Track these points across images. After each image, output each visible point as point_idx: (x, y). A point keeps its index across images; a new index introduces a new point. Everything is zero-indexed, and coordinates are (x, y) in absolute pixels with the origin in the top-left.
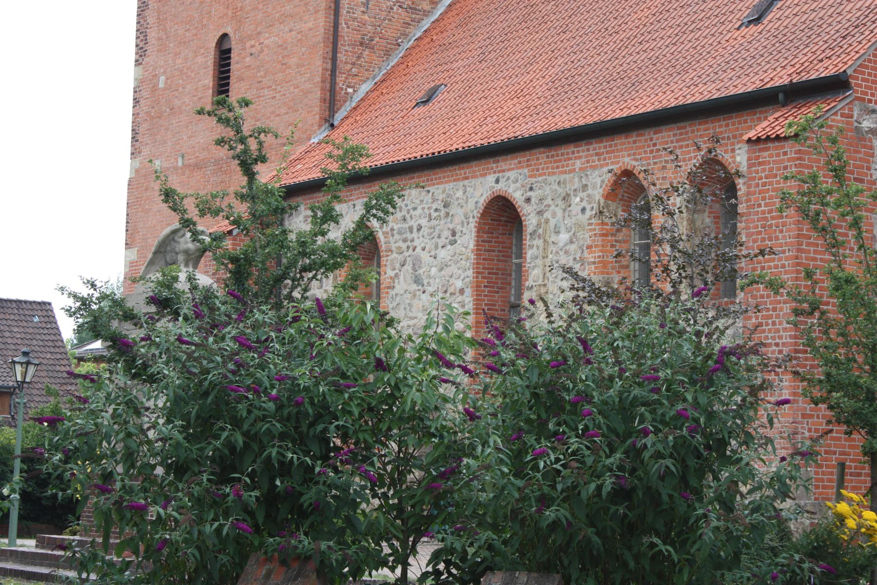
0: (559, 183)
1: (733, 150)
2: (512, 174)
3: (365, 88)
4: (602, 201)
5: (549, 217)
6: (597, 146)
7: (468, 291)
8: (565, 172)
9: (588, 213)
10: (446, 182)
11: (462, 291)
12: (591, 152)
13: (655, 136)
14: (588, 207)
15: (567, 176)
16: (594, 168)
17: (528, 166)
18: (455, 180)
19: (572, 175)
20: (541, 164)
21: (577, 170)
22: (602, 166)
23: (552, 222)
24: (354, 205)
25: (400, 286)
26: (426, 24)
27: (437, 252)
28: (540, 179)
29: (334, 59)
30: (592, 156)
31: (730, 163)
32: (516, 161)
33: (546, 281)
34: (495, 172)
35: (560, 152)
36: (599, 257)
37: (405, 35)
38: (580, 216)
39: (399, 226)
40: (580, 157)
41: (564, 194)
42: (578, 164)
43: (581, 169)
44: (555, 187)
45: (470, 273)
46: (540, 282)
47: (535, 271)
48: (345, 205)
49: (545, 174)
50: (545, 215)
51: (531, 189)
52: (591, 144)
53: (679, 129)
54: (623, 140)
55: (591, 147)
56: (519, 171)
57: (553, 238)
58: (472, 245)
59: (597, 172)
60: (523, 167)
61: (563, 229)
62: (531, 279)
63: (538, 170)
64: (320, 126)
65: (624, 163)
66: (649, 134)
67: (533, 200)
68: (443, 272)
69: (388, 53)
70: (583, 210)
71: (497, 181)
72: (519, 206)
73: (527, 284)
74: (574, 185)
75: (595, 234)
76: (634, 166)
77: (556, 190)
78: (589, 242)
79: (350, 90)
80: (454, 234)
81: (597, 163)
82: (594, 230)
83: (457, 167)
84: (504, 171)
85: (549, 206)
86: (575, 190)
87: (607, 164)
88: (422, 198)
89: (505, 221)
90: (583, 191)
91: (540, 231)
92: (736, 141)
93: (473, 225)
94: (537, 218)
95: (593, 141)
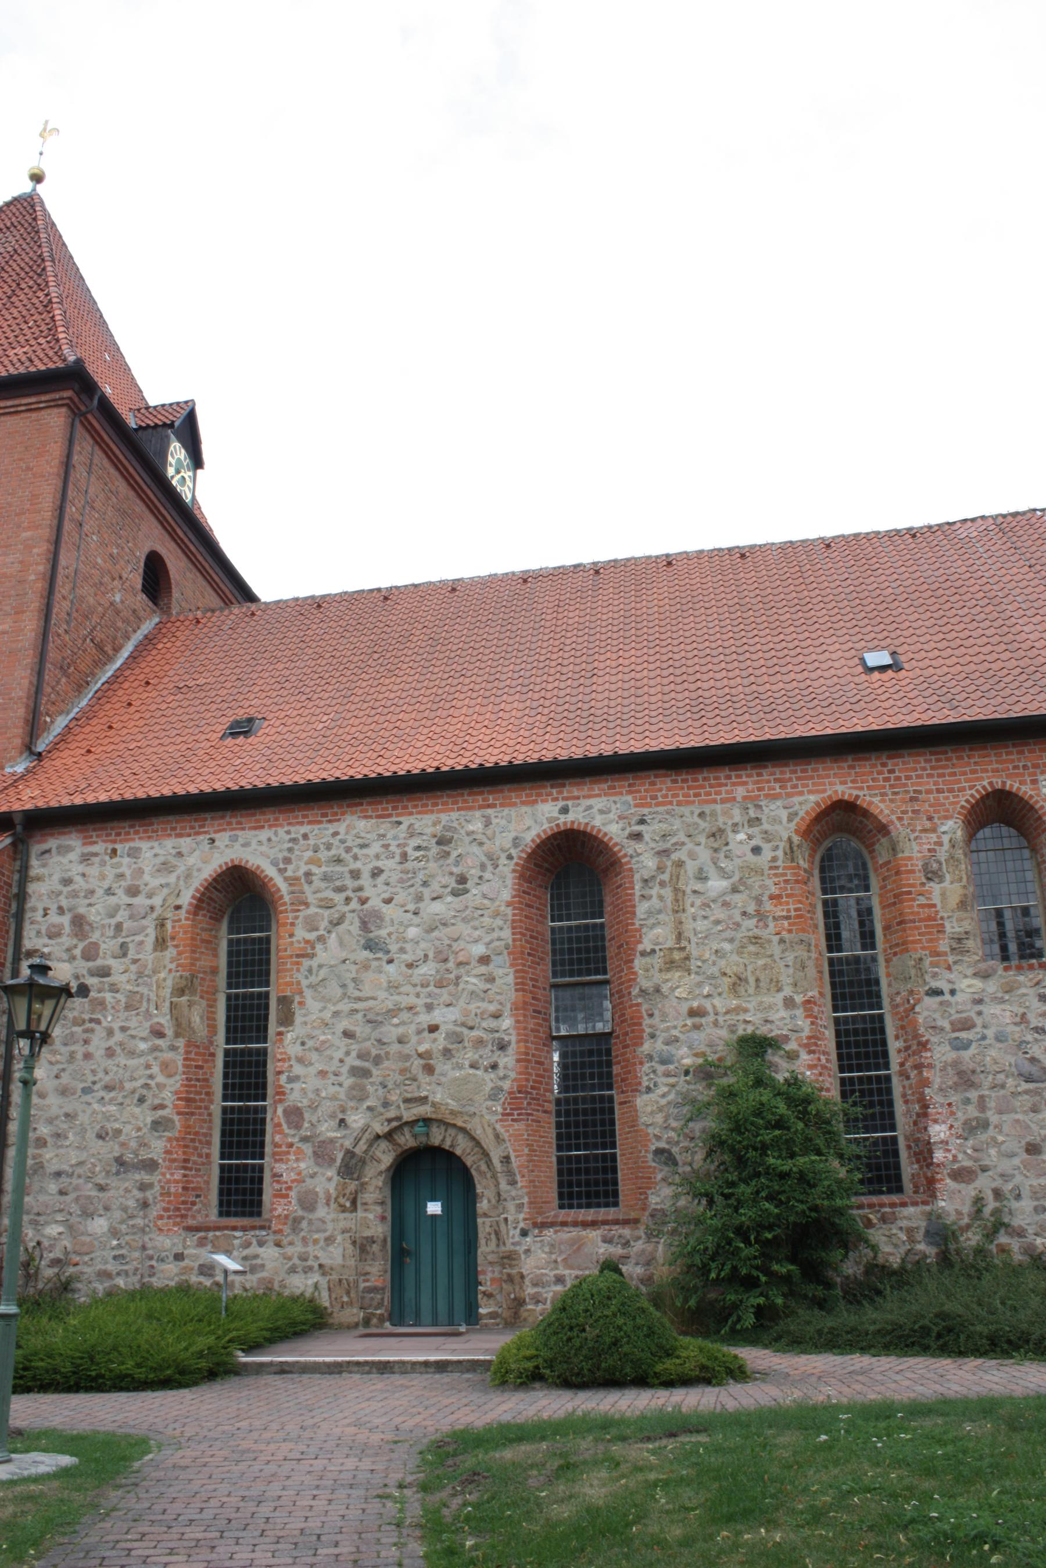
0: (702, 815)
1: (1034, 782)
2: (599, 803)
3: (61, 723)
4: (796, 839)
5: (683, 858)
6: (777, 770)
7: (505, 958)
8: (715, 801)
9: (767, 854)
10: (440, 811)
11: (484, 960)
12: (766, 777)
13: (890, 762)
14: (766, 847)
15: (718, 807)
16: (775, 797)
17: (629, 792)
18: (459, 809)
19: (728, 805)
20: (661, 790)
21: (739, 799)
22: (789, 795)
23: (691, 867)
24: (213, 841)
25: (328, 954)
26: (110, 671)
27: (421, 905)
28: (661, 809)
29: (40, 673)
30: (769, 781)
31: (1031, 797)
32: (605, 786)
33: (684, 944)
34: (556, 799)
35: (700, 777)
36: (796, 910)
37: (93, 674)
38: (751, 857)
39: (324, 869)
40: (745, 783)
41: (714, 829)
42: (740, 792)
43: (745, 798)
44: (696, 819)
45: (507, 934)
46: (670, 943)
47: (658, 930)
48: (188, 840)
49: (671, 803)
50: (674, 856)
51: (642, 822)
52: (765, 767)
53: (932, 754)
54: (829, 764)
55: (764, 772)
56: (612, 798)
57: (698, 887)
58: (506, 895)
59: (779, 803)
60: (621, 794)
61: (711, 871)
62: (645, 940)
63: (654, 798)
64: (21, 753)
65: (836, 792)
66: (877, 758)
67: (647, 837)
68: (436, 934)
69: (80, 687)
70: (756, 850)
71: (565, 810)
72: (616, 844)
73: (640, 947)
74: (732, 818)
75: (786, 881)
76: (857, 797)
77: (696, 824)
78: (774, 890)
79: (48, 719)
80: (462, 880)
81: (778, 790)
82: (785, 875)
83: (466, 792)
84: (578, 798)
85: (683, 844)
86: (735, 825)
87: (801, 793)
88: (382, 832)
89: (547, 870)
90: (750, 826)
91: (666, 877)
92: (1038, 771)
93: (507, 870)
94: (656, 860)
95: (791, 762)
